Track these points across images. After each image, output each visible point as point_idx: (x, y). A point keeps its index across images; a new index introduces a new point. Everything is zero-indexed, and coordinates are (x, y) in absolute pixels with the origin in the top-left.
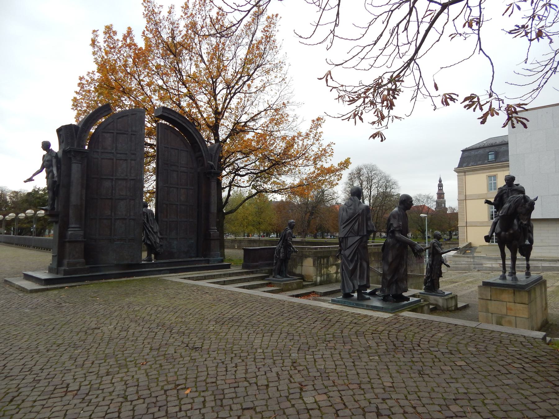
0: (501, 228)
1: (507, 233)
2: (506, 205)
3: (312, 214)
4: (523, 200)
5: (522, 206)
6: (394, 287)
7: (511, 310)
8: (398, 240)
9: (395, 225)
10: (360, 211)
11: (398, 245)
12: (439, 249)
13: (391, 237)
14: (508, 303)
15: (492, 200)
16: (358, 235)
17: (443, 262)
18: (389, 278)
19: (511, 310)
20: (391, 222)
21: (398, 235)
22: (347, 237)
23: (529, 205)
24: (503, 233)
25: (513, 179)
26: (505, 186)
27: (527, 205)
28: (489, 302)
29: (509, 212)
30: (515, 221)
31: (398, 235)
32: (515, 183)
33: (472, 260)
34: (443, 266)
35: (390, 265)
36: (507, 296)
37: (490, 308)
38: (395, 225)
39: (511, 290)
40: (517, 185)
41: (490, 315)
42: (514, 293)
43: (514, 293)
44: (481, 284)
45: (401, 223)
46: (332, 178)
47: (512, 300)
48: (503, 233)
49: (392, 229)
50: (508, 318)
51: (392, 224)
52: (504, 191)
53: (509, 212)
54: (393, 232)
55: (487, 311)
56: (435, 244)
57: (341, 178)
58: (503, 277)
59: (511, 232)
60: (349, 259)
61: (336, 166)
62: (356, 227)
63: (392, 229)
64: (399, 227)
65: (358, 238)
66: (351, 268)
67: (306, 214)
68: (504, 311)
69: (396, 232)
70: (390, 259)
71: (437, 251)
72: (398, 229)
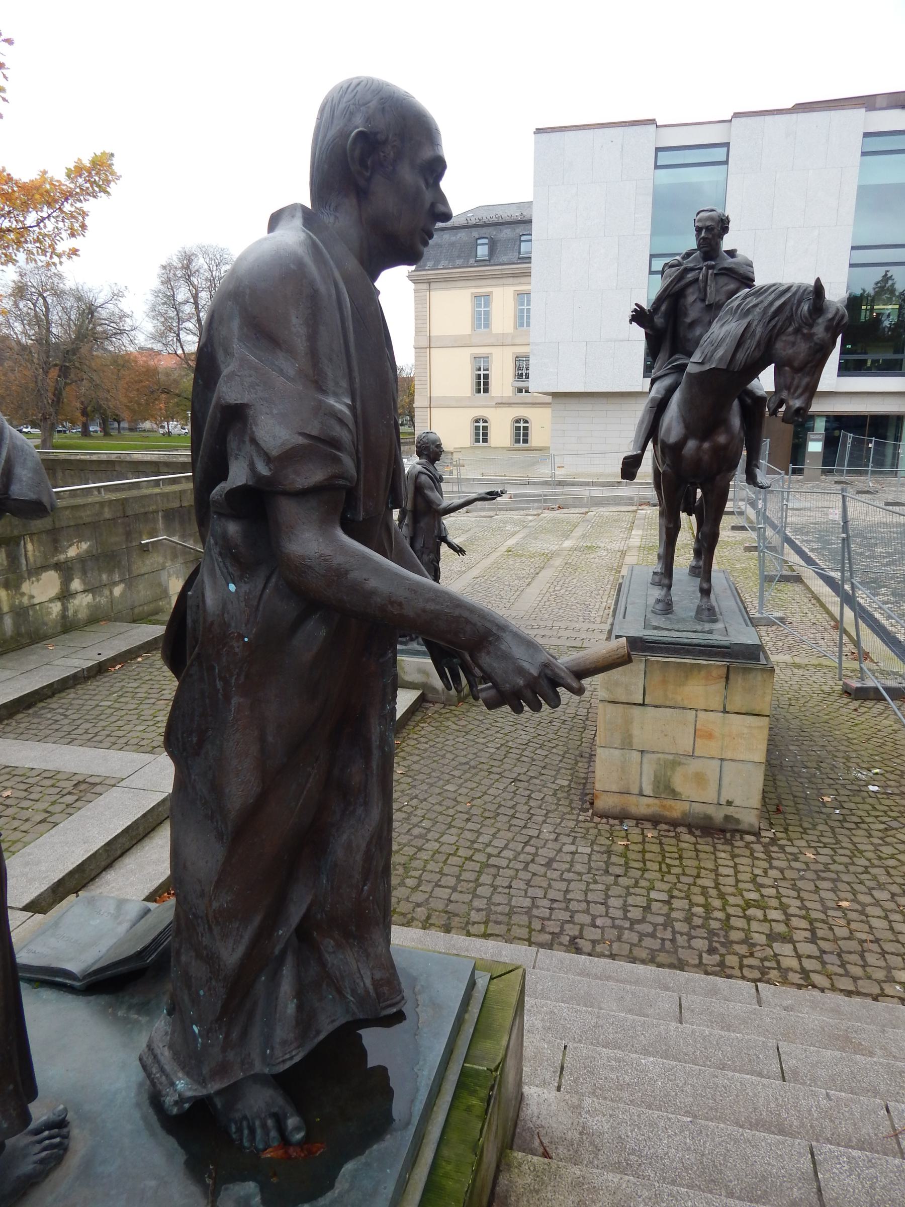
0: (687, 426)
1: (706, 445)
3: (64, 371)
4: (805, 307)
5: (797, 331)
6: (286, 987)
7: (710, 736)
8: (320, 599)
9: (274, 430)
11: (314, 634)
12: (433, 495)
13: (240, 562)
14: (701, 715)
17: (444, 539)
19: (710, 736)
20: (230, 391)
21: (314, 542)
23: (827, 329)
24: (691, 444)
25: (722, 225)
26: (688, 255)
28: (637, 711)
29: (741, 356)
31: (314, 542)
32: (727, 243)
33: (456, 489)
34: (444, 548)
35: (240, 833)
36: (701, 691)
37: (636, 731)
38: (274, 430)
39: (717, 664)
40: (732, 253)
41: (636, 756)
42: (727, 678)
43: (727, 678)
45: (340, 405)
46: (50, 225)
47: (716, 702)
49: (238, 475)
50: (694, 766)
51: (236, 416)
52: (690, 276)
54: (257, 505)
55: (627, 744)
56: (424, 478)
57: (83, 227)
58: (667, 607)
59: (722, 439)
61: (58, 174)
63: (238, 475)
64: (322, 446)
67: (46, 373)
68: (685, 743)
69: (288, 510)
70: (239, 790)
71: (429, 503)
72: (312, 475)
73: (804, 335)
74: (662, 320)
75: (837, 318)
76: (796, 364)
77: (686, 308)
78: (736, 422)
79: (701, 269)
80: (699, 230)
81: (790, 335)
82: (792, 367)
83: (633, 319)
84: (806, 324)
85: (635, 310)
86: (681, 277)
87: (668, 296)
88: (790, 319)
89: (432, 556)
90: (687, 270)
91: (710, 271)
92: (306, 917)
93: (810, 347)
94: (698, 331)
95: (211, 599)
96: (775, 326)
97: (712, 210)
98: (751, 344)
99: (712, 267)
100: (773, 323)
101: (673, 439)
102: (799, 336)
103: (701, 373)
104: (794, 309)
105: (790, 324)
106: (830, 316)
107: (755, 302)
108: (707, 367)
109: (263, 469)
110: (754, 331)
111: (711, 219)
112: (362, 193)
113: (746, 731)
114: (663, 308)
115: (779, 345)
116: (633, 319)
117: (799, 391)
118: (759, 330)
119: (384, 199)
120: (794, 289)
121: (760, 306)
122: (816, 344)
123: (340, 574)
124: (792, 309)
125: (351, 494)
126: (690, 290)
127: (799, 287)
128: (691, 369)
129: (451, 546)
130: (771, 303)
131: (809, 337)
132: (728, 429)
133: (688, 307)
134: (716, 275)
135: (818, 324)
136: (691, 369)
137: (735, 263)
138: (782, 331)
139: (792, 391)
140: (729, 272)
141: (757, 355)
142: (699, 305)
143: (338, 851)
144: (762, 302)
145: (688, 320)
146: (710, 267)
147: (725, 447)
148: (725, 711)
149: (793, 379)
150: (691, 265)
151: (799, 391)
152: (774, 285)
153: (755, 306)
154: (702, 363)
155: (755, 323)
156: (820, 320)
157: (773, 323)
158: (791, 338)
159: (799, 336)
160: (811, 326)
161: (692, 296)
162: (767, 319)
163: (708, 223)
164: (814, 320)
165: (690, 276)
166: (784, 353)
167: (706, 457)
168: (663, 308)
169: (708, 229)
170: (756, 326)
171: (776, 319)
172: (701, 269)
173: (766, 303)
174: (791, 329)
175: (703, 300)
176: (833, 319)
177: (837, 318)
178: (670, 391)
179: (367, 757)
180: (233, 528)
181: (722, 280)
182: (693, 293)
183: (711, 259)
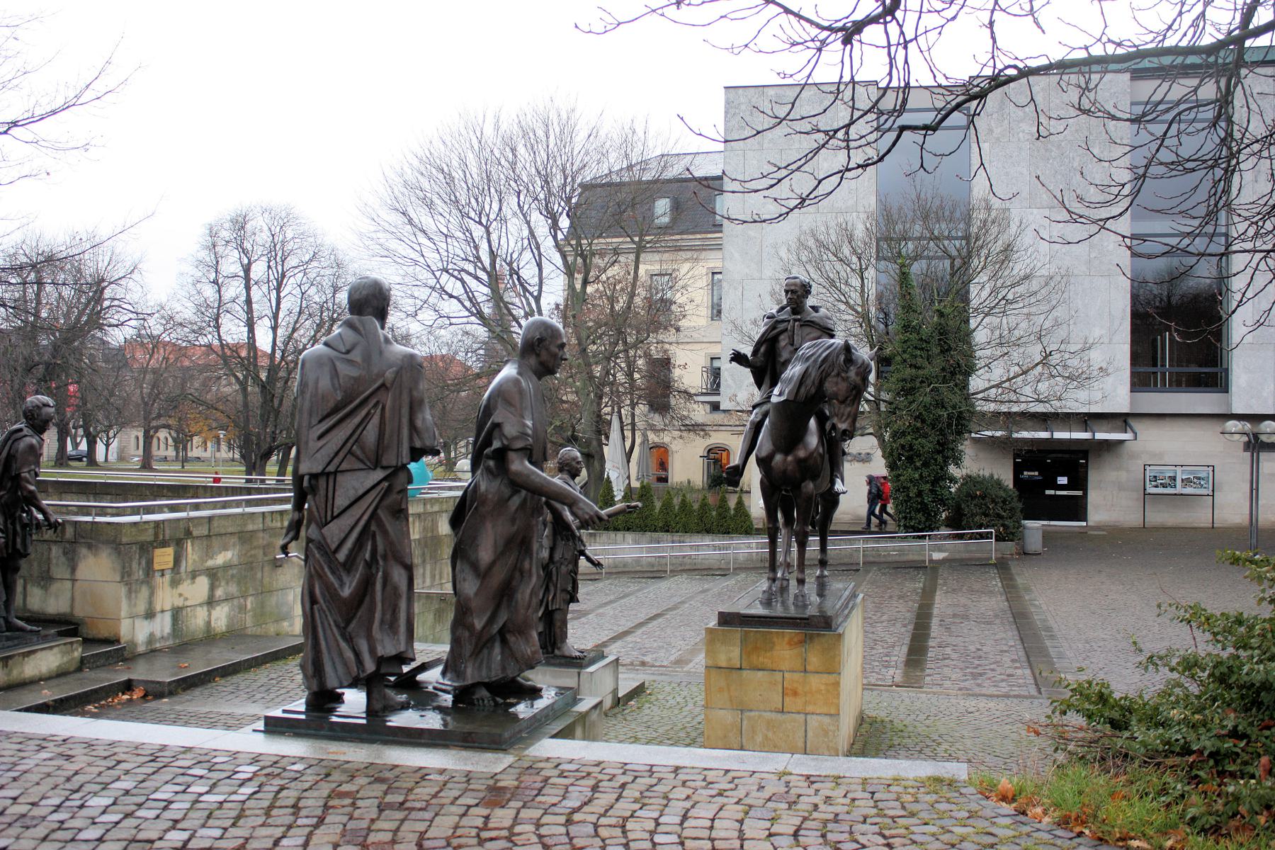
1: (790, 458)
2: (794, 371)
4: (842, 358)
5: (838, 375)
10: (389, 374)
15: (747, 350)
16: (377, 464)
17: (582, 553)
18: (479, 624)
19: (795, 694)
21: (520, 465)
22: (336, 473)
23: (857, 374)
24: (778, 457)
25: (805, 289)
27: (852, 373)
30: (812, 422)
31: (520, 465)
32: (810, 301)
40: (815, 309)
44: (713, 623)
48: (778, 457)
51: (497, 426)
52: (782, 327)
53: (803, 390)
59: (801, 453)
60: (342, 556)
62: (371, 434)
63: (496, 444)
65: (379, 475)
66: (346, 592)
69: (512, 455)
70: (485, 554)
72: (519, 445)
78: (813, 440)
80: (787, 292)
83: (732, 360)
86: (773, 327)
89: (570, 567)
92: (504, 625)
95: (483, 487)
101: (764, 454)
108: (782, 399)
109: (505, 442)
111: (795, 285)
112: (538, 355)
113: (823, 687)
114: (762, 349)
116: (732, 360)
119: (544, 356)
123: (528, 476)
125: (531, 450)
126: (782, 337)
128: (774, 399)
129: (589, 559)
131: (845, 379)
132: (805, 447)
136: (774, 399)
138: (828, 375)
140: (811, 324)
143: (519, 596)
145: (782, 360)
146: (795, 320)
147: (805, 460)
148: (805, 671)
154: (780, 395)
161: (783, 341)
167: (790, 468)
168: (762, 349)
169: (792, 292)
178: (765, 415)
179: (531, 559)
180: (491, 463)
181: (807, 330)
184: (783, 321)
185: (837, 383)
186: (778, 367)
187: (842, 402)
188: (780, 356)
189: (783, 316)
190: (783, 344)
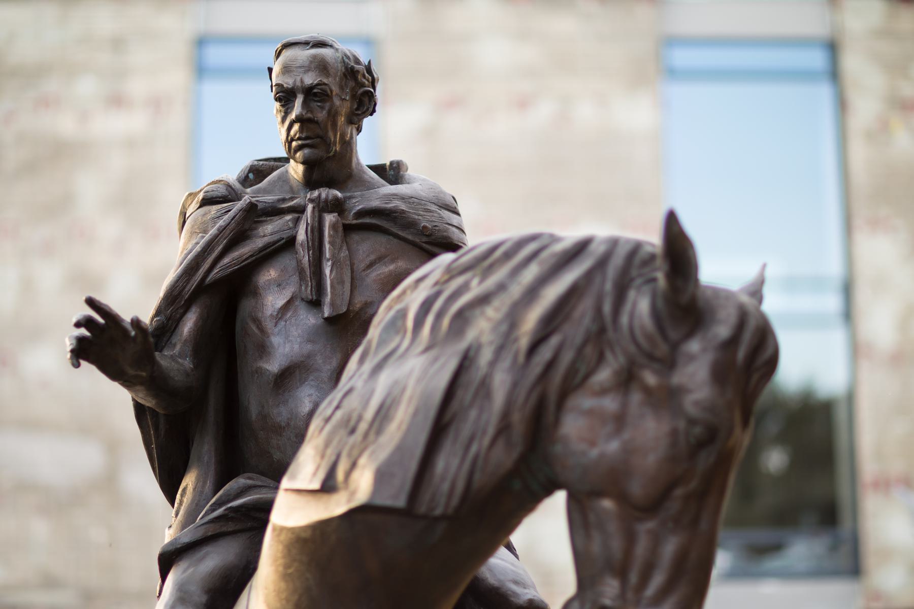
4: (641, 305)
23: (721, 374)
26: (257, 173)
27: (695, 373)
32: (371, 145)
40: (391, 173)
52: (269, 231)
53: (449, 464)
73: (647, 391)
74: (188, 363)
75: (747, 337)
76: (637, 489)
77: (262, 330)
79: (300, 210)
80: (285, 97)
81: (603, 392)
82: (622, 498)
83: (82, 352)
84: (651, 357)
85: (86, 323)
86: (239, 233)
87: (201, 289)
88: (599, 337)
90: (254, 214)
91: (329, 219)
93: (674, 433)
94: (304, 397)
96: (550, 365)
97: (321, 44)
98: (480, 421)
99: (337, 206)
100: (545, 353)
102: (636, 397)
103: (321, 528)
104: (607, 308)
105: (601, 359)
106: (723, 331)
107: (476, 289)
110: (485, 387)
115: (573, 426)
116: (82, 352)
117: (657, 581)
118: (501, 383)
120: (597, 249)
121: (496, 303)
122: (692, 422)
124: (598, 310)
126: (269, 274)
127: (614, 243)
130: (532, 293)
131: (667, 398)
133: (269, 325)
134: (348, 229)
135: (692, 358)
137: (403, 198)
138: (573, 383)
139: (633, 578)
141: (504, 458)
142: (308, 319)
144: (501, 287)
145: (273, 366)
146: (323, 207)
149: (630, 538)
150: (269, 198)
151: (657, 581)
152: (533, 238)
153: (483, 300)
155: (486, 356)
156: (694, 346)
157: (545, 353)
158: (610, 404)
159: (636, 397)
160: (669, 363)
161: (274, 292)
162: (524, 342)
163: (310, 79)
164: (675, 347)
165: (269, 231)
166: (594, 453)
169: (309, 92)
170: (493, 363)
171: (554, 341)
172: (300, 210)
173: (516, 290)
174: (604, 375)
175: (315, 304)
176: (733, 342)
177: (747, 337)
181: (366, 247)
182: (280, 285)
183: (330, 184)
184: (274, 211)
185: (620, 421)
186: (253, 401)
187: (651, 507)
188: (263, 349)
189: (263, 194)
190: (274, 301)
